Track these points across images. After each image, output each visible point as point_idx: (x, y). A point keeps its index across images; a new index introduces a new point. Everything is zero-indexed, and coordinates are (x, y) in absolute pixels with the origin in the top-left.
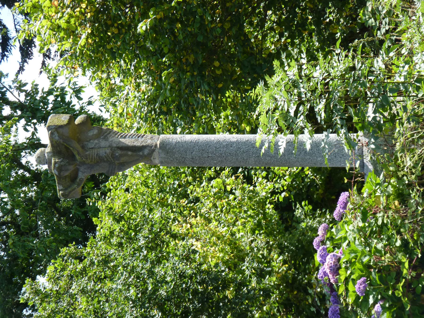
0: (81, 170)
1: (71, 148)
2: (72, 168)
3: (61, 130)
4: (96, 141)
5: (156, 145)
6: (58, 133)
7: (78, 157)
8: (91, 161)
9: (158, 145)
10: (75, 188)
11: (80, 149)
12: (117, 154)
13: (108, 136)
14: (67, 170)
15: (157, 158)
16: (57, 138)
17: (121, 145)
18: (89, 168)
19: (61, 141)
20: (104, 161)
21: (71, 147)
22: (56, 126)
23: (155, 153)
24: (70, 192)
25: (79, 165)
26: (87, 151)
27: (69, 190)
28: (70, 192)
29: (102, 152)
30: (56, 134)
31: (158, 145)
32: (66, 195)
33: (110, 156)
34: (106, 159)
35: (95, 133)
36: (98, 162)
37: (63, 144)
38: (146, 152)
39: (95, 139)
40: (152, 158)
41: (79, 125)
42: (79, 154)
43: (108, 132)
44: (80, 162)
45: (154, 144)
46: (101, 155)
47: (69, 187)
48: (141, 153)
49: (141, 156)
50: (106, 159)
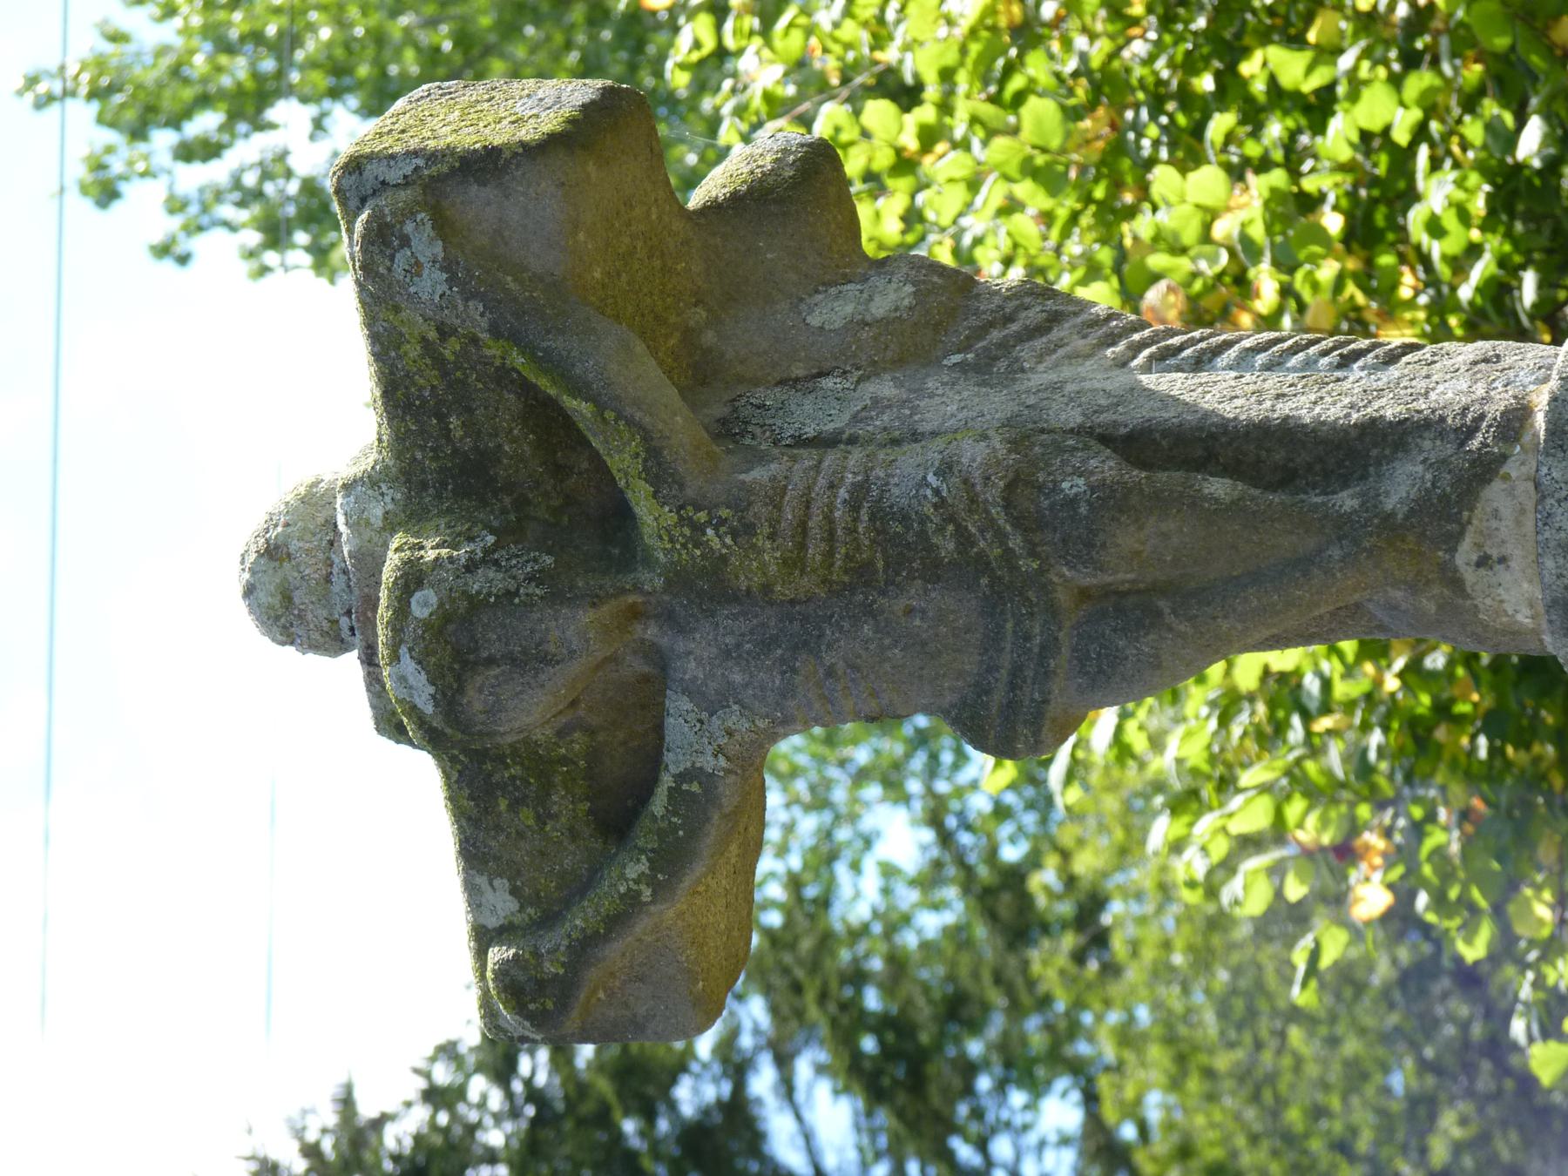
0: (691, 669)
1: (580, 408)
2: (578, 630)
3: (476, 204)
4: (885, 388)
5: (1518, 416)
6: (443, 226)
7: (650, 515)
8: (794, 563)
9: (1540, 421)
10: (631, 905)
11: (681, 427)
12: (1072, 486)
13: (1025, 352)
14: (531, 660)
15: (1520, 557)
16: (431, 284)
17: (1134, 416)
18: (767, 645)
19: (476, 317)
20: (934, 571)
21: (580, 389)
22: (433, 157)
23: (1494, 494)
24: (584, 948)
25: (668, 618)
26: (762, 459)
27: (579, 920)
28: (584, 948)
29: (909, 475)
30: (425, 244)
31: (1540, 421)
32: (541, 985)
33: (993, 494)
34: (947, 546)
35: (880, 307)
36: (862, 573)
37: (503, 376)
38: (1402, 484)
39: (874, 370)
40: (1465, 554)
41: (713, 209)
42: (659, 474)
43: (1034, 315)
44: (679, 580)
45: (1494, 410)
46: (899, 494)
47: (580, 887)
48: (1347, 501)
49: (1343, 527)
50: (947, 546)
